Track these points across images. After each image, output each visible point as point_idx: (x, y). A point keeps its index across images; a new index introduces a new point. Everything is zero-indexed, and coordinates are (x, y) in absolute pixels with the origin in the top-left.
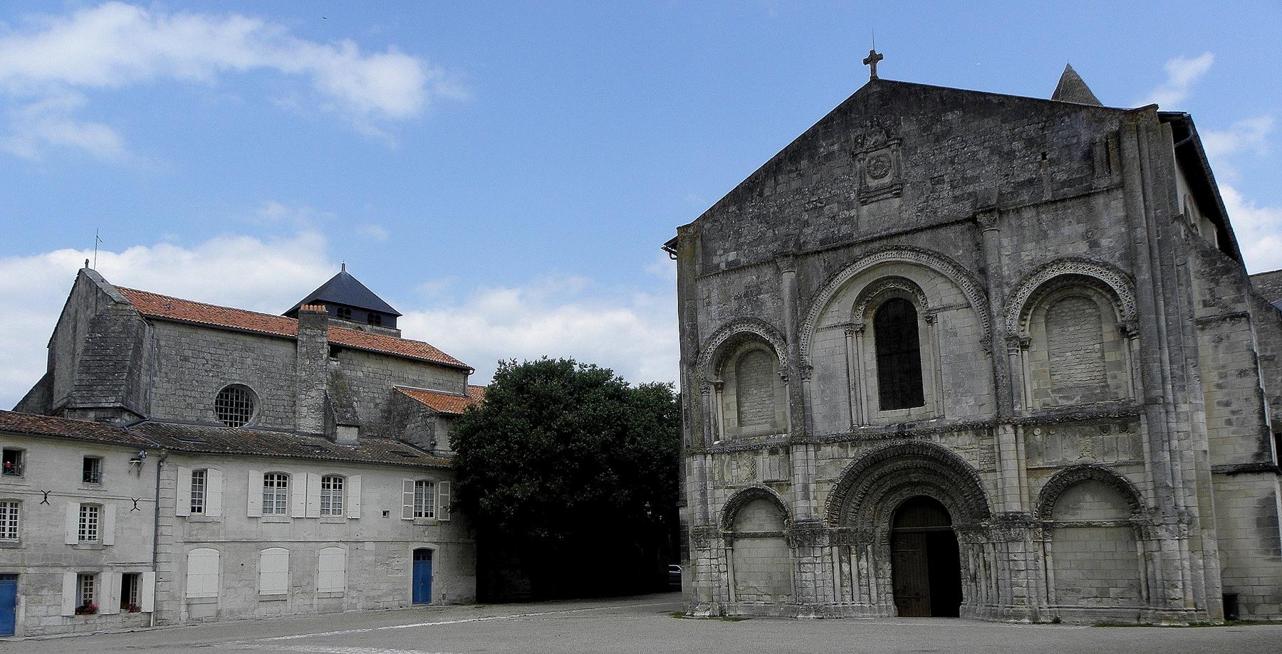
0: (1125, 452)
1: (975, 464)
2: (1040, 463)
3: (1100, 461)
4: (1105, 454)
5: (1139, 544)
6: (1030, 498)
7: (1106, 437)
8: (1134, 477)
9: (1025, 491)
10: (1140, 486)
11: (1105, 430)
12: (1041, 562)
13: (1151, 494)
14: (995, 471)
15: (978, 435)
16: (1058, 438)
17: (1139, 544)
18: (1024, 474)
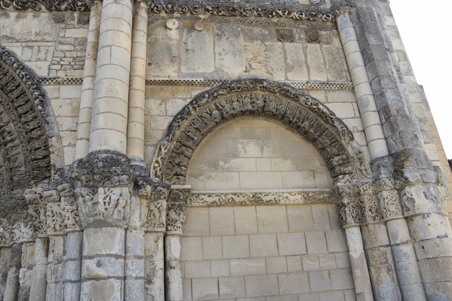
0: (318, 69)
1: (41, 69)
2: (170, 72)
3: (279, 77)
4: (288, 68)
5: (354, 235)
6: (146, 135)
7: (287, 45)
8: (341, 108)
9: (138, 116)
10: (353, 124)
11: (284, 37)
12: (159, 282)
13: (376, 132)
14: (79, 81)
15: (59, 20)
16: (208, 38)
17: (354, 235)
18: (139, 84)
